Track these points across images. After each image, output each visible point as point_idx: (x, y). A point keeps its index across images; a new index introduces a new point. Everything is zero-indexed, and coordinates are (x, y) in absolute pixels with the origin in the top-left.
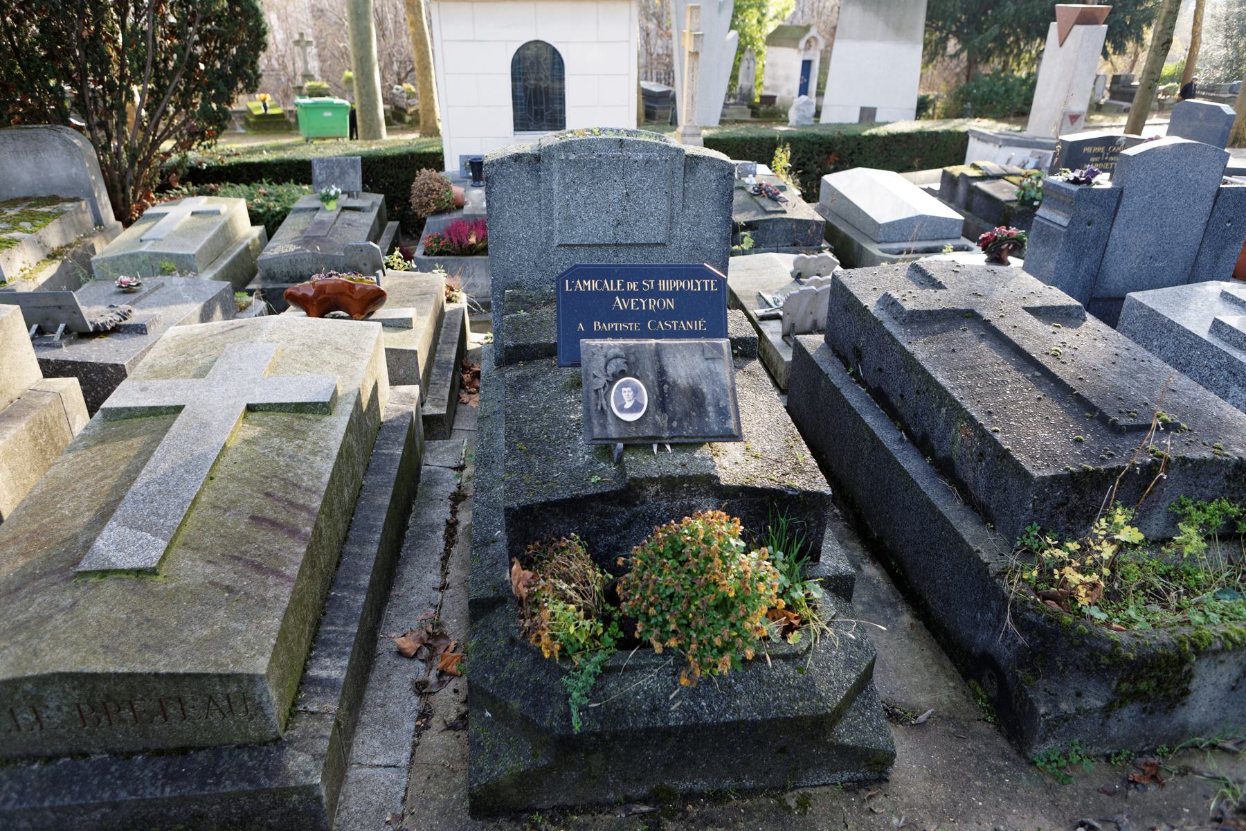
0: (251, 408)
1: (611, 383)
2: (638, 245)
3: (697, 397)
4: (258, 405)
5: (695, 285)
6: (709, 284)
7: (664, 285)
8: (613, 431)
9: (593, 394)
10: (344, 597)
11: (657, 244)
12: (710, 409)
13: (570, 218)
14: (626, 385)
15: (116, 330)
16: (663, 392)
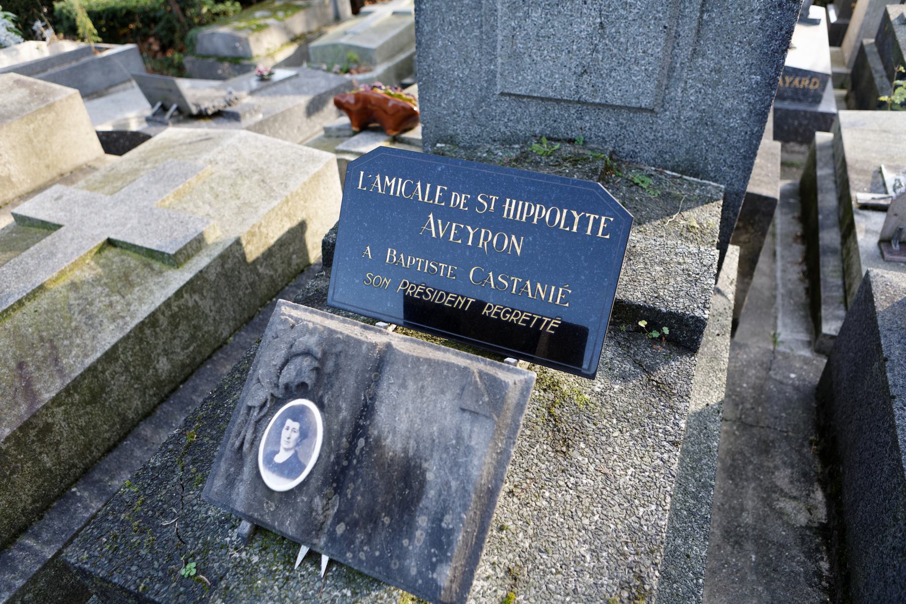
0: (110, 243)
1: (278, 402)
2: (614, 107)
3: (408, 485)
4: (119, 242)
5: (570, 220)
6: (597, 223)
7: (512, 208)
8: (241, 496)
9: (243, 411)
10: (80, 499)
11: (640, 109)
12: (423, 521)
13: (515, 55)
14: (298, 414)
15: (218, 115)
16: (349, 459)
